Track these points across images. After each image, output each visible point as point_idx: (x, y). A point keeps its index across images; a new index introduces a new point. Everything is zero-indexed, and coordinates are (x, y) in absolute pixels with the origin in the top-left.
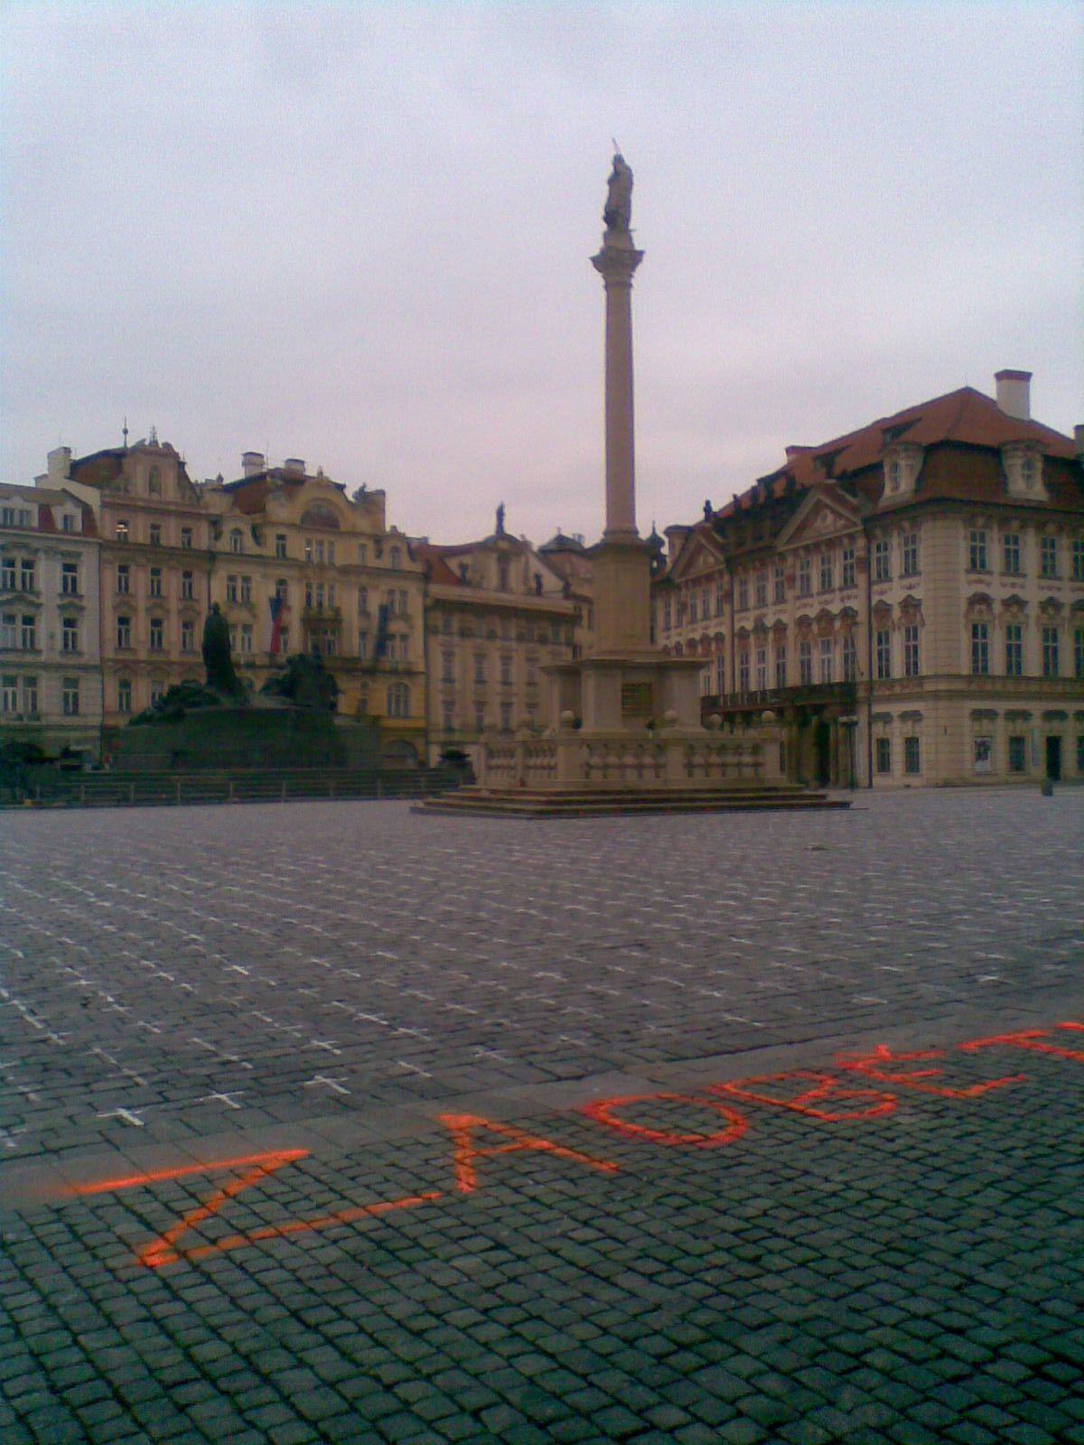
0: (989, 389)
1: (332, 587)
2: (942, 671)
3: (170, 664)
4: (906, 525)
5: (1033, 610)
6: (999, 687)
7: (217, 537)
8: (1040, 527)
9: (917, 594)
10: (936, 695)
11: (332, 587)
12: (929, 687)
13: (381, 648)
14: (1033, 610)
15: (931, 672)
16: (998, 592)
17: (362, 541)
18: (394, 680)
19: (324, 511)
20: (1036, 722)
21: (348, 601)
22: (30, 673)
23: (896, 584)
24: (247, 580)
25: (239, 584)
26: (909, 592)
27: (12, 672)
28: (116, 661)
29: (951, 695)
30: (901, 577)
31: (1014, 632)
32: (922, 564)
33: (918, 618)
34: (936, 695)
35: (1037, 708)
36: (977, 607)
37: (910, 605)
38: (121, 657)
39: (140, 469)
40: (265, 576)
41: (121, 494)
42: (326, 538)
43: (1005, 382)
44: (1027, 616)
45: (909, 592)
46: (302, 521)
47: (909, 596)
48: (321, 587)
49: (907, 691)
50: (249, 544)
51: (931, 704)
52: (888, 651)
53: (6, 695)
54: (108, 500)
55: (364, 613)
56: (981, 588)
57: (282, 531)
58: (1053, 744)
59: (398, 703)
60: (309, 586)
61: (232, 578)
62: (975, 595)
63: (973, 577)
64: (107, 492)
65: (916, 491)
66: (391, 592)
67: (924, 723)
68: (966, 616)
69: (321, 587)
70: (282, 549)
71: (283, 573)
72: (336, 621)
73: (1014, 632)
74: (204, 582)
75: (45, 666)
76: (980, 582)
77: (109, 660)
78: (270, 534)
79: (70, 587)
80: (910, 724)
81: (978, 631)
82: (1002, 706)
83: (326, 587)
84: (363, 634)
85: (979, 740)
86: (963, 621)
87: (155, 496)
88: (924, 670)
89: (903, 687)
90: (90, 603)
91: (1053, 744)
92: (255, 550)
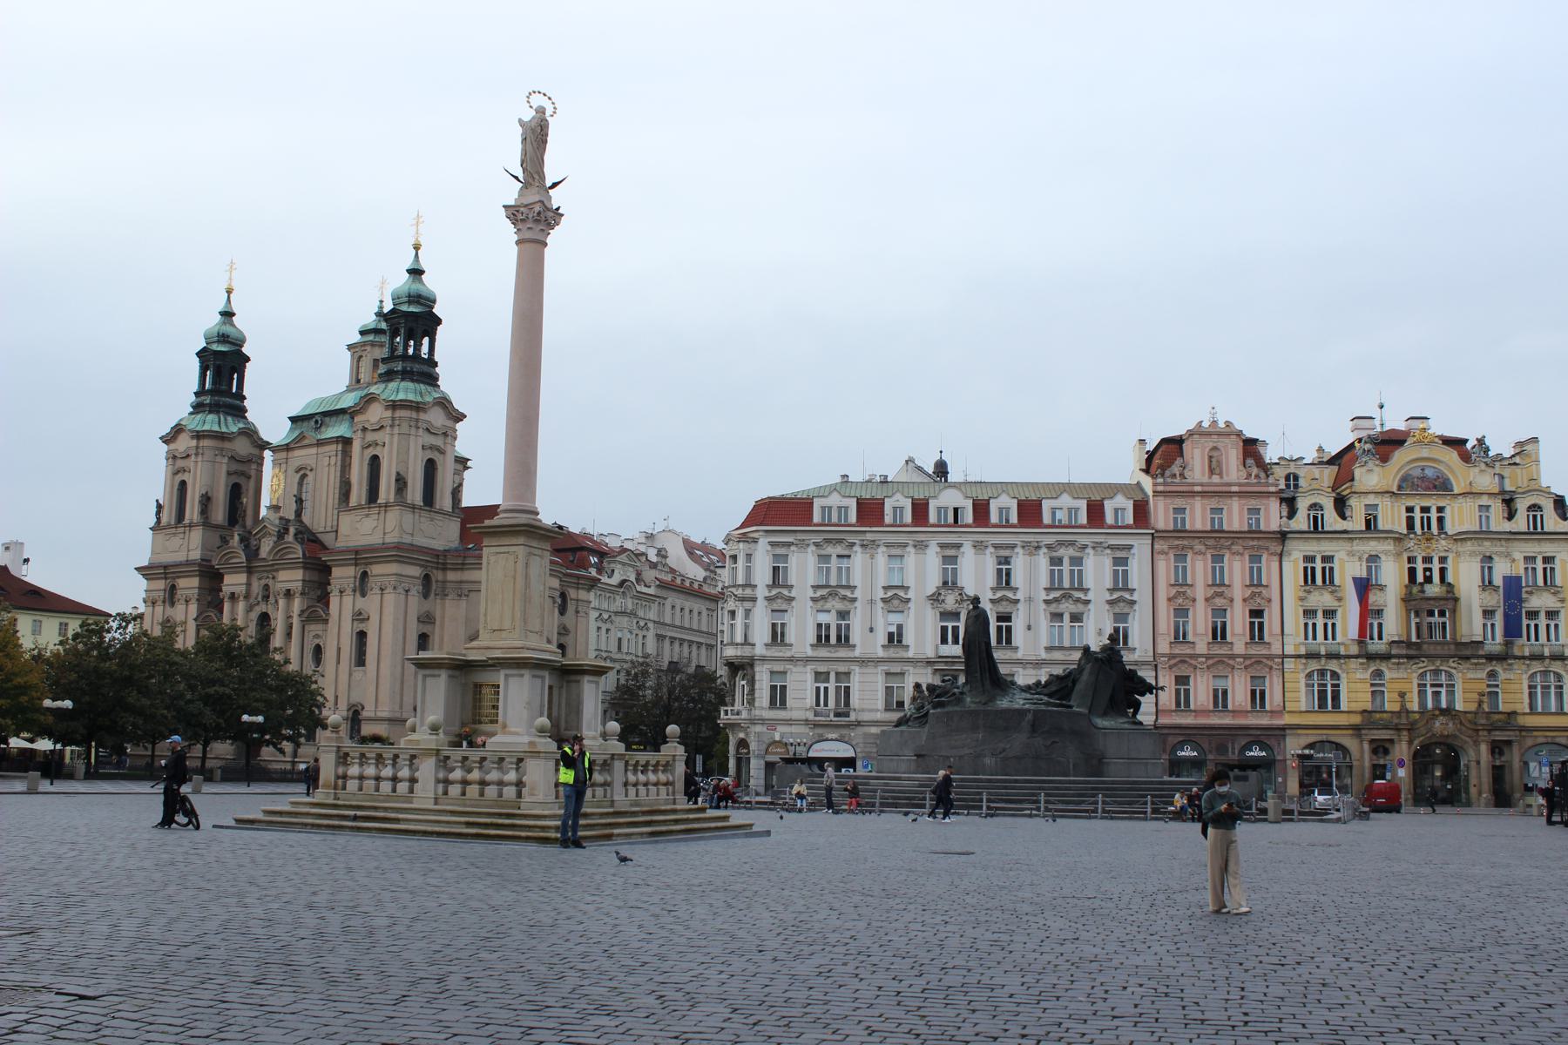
1: (1443, 560)
3: (1233, 657)
7: (1292, 513)
11: (1443, 560)
13: (1512, 630)
17: (1485, 501)
18: (1537, 667)
19: (1429, 473)
21: (1465, 575)
22: (842, 668)
24: (1327, 559)
25: (1319, 565)
27: (822, 668)
28: (1171, 656)
38: (1177, 651)
39: (1197, 452)
40: (1351, 554)
41: (1177, 480)
42: (1432, 503)
46: (1400, 488)
48: (1428, 560)
50: (1331, 520)
53: (818, 689)
54: (1160, 488)
55: (1487, 585)
57: (1371, 500)
59: (1546, 695)
60: (1411, 560)
61: (1309, 559)
64: (1160, 480)
66: (1530, 559)
69: (1428, 560)
70: (1370, 523)
71: (1373, 547)
72: (1451, 599)
74: (1275, 565)
75: (863, 662)
77: (1163, 655)
78: (1357, 507)
79: (1120, 585)
83: (1436, 560)
84: (1488, 613)
87: (1216, 479)
90: (1142, 596)
92: (1341, 525)
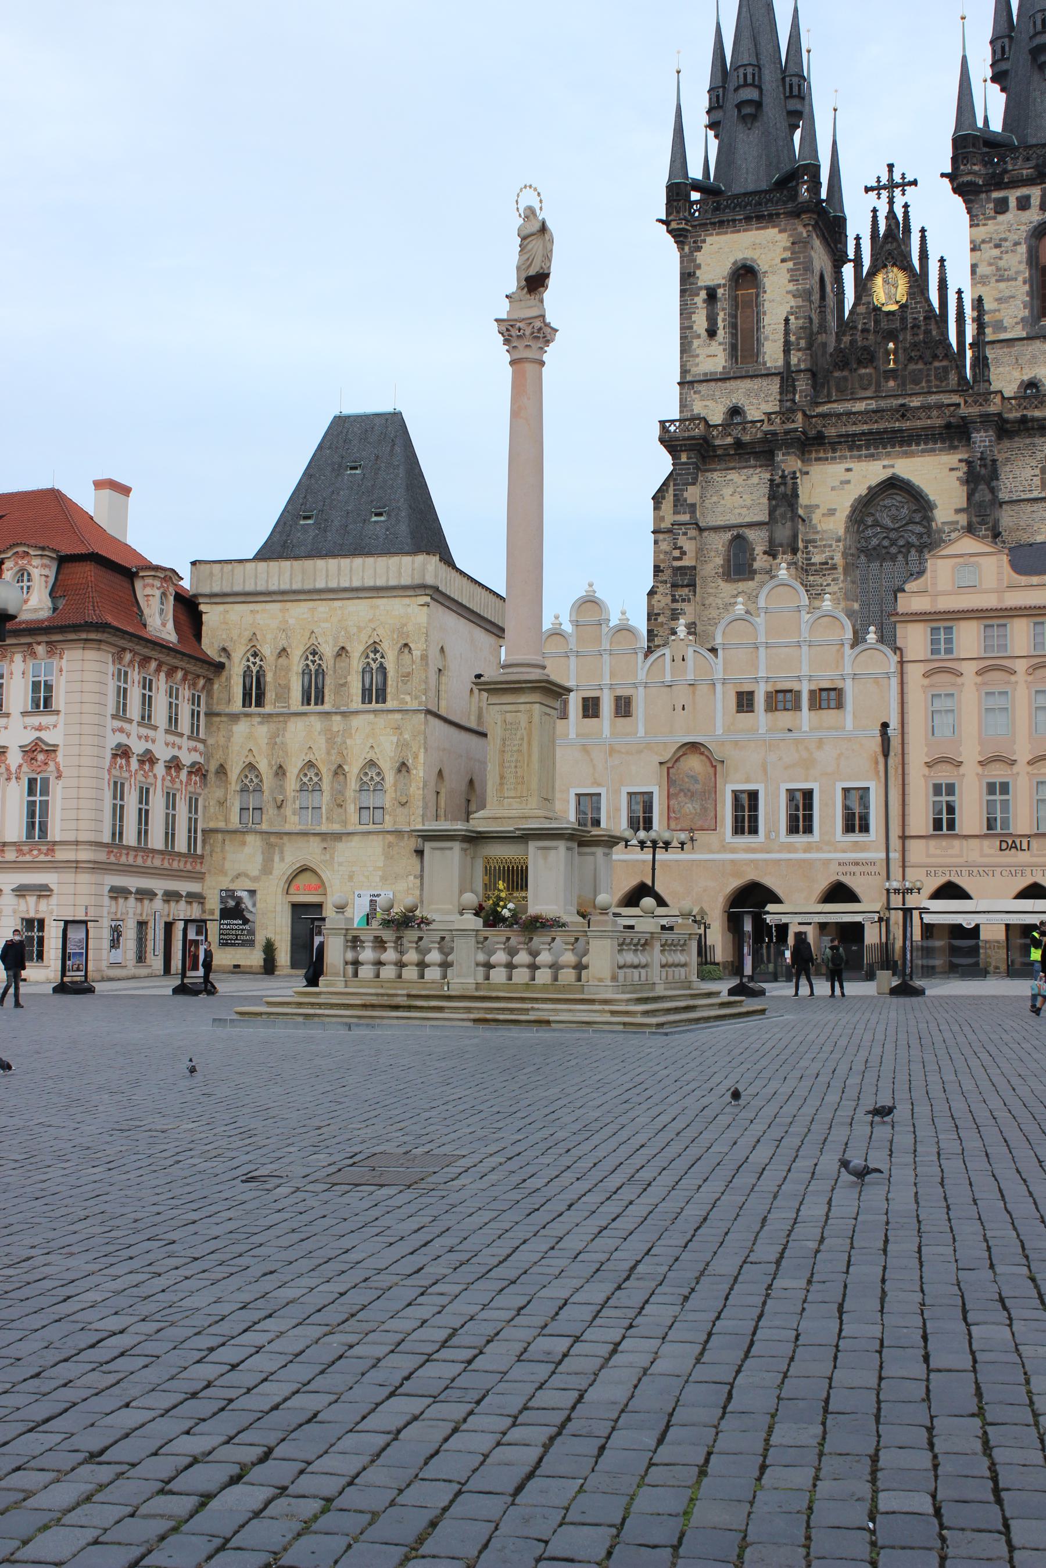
0: (84, 498)
2: (82, 837)
4: (41, 650)
5: (160, 769)
6: (157, 862)
8: (171, 673)
9: (49, 737)
10: (76, 866)
12: (61, 855)
14: (160, 769)
15: (70, 837)
16: (138, 747)
20: (158, 904)
23: (16, 721)
26: (37, 734)
29: (97, 867)
30: (25, 714)
31: (144, 795)
32: (59, 701)
33: (52, 766)
34: (76, 866)
35: (159, 885)
36: (119, 760)
37: (38, 751)
43: (107, 492)
44: (155, 776)
45: (37, 734)
47: (39, 738)
49: (28, 858)
51: (69, 877)
52: (45, 805)
56: (122, 739)
58: (169, 927)
62: (119, 746)
63: (118, 724)
65: (55, 609)
67: (53, 900)
68: (109, 771)
73: (144, 795)
76: (121, 730)
80: (32, 900)
81: (118, 790)
82: (133, 883)
85: (113, 924)
86: (107, 777)
88: (56, 832)
89: (20, 851)
91: (169, 927)
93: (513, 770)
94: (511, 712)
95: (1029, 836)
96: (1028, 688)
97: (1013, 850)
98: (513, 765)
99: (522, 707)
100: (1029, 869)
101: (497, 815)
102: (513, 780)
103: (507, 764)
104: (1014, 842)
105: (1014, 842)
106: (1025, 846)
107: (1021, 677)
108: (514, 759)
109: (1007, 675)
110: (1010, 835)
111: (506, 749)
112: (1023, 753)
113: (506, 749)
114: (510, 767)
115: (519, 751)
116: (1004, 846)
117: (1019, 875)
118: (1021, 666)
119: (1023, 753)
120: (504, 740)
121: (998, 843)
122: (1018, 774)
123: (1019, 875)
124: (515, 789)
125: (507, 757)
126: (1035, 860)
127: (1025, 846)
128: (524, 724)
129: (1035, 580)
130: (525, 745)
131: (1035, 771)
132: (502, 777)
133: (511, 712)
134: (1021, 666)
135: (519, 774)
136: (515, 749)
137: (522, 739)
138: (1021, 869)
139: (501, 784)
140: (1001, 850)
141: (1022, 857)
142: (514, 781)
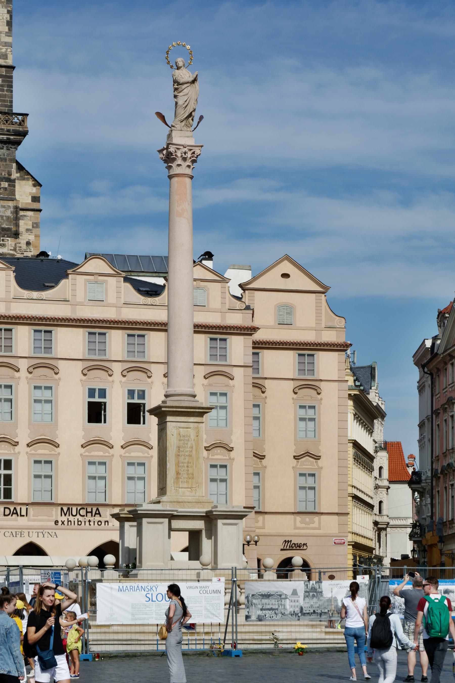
93: (186, 469)
94: (183, 428)
95: (27, 504)
96: (28, 383)
97: (14, 516)
98: (186, 465)
99: (191, 425)
100: (26, 531)
101: (180, 500)
102: (185, 476)
103: (181, 465)
104: (15, 509)
105: (15, 509)
106: (24, 513)
107: (23, 373)
108: (186, 461)
109: (13, 371)
110: (12, 503)
111: (181, 453)
112: (23, 436)
113: (181, 453)
114: (183, 466)
115: (190, 456)
116: (7, 512)
117: (19, 536)
118: (23, 365)
119: (23, 436)
120: (179, 447)
121: (3, 509)
122: (19, 453)
123: (19, 536)
124: (187, 482)
125: (181, 459)
126: (31, 523)
127: (24, 513)
128: (193, 437)
129: (35, 294)
130: (194, 452)
131: (33, 452)
132: (178, 473)
133: (183, 428)
134: (23, 365)
135: (190, 472)
136: (187, 454)
137: (192, 447)
138: (19, 531)
139: (177, 478)
140: (5, 515)
141: (22, 521)
142: (187, 476)
